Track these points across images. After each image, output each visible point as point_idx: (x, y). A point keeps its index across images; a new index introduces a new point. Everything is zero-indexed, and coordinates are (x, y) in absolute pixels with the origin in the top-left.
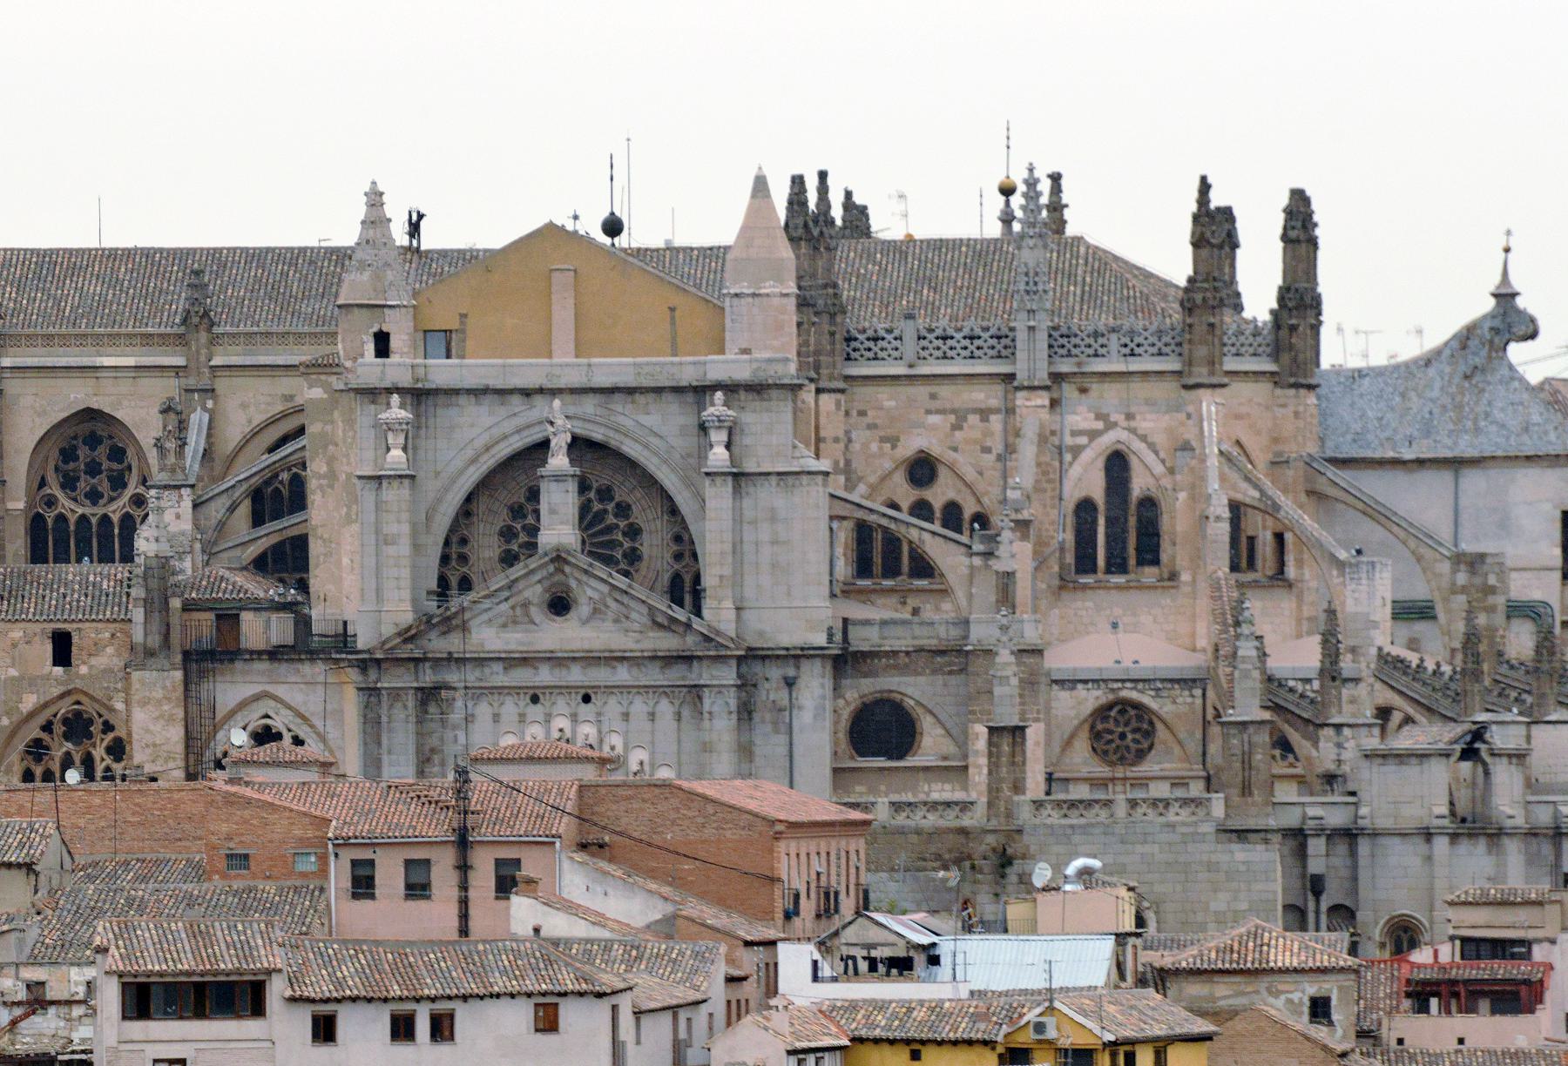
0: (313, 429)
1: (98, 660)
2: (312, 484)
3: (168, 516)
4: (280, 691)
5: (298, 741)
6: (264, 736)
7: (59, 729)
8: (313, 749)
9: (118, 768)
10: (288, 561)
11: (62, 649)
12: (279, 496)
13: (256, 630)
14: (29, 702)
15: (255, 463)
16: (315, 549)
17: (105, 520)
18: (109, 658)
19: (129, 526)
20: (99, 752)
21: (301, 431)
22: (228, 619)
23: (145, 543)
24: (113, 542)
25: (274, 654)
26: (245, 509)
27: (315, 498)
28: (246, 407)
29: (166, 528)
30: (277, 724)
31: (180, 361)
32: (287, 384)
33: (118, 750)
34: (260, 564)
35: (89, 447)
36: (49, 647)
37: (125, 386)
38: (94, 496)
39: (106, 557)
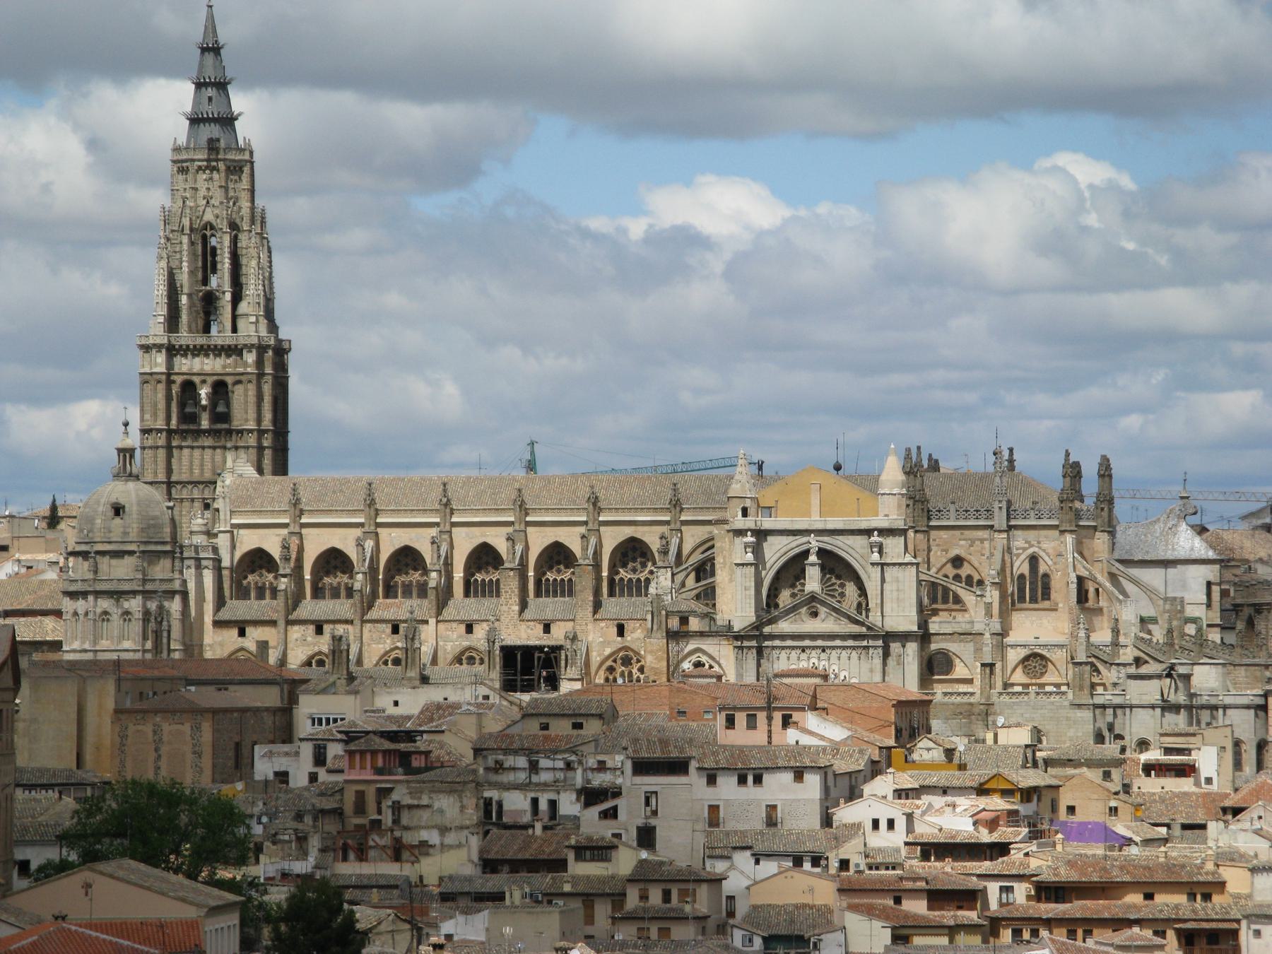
0: (718, 545)
1: (635, 636)
2: (717, 566)
3: (662, 579)
4: (704, 647)
5: (711, 667)
6: (698, 665)
7: (619, 662)
8: (716, 668)
9: (642, 677)
10: (708, 595)
11: (621, 631)
12: (704, 570)
13: (695, 624)
14: (608, 651)
15: (697, 557)
16: (718, 591)
17: (639, 580)
18: (639, 634)
19: (648, 581)
20: (635, 671)
21: (713, 547)
22: (684, 620)
23: (652, 590)
24: (639, 588)
25: (702, 634)
26: (693, 575)
27: (718, 572)
28: (692, 537)
29: (662, 582)
30: (704, 659)
31: (668, 518)
32: (708, 528)
33: (641, 670)
34: (698, 597)
35: (633, 551)
36: (615, 629)
37: (646, 528)
38: (634, 570)
39: (639, 594)
